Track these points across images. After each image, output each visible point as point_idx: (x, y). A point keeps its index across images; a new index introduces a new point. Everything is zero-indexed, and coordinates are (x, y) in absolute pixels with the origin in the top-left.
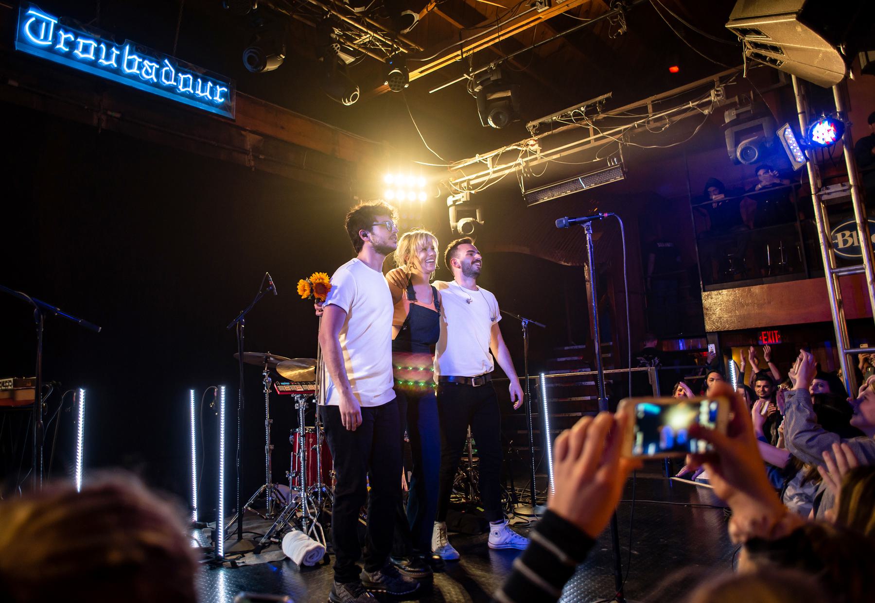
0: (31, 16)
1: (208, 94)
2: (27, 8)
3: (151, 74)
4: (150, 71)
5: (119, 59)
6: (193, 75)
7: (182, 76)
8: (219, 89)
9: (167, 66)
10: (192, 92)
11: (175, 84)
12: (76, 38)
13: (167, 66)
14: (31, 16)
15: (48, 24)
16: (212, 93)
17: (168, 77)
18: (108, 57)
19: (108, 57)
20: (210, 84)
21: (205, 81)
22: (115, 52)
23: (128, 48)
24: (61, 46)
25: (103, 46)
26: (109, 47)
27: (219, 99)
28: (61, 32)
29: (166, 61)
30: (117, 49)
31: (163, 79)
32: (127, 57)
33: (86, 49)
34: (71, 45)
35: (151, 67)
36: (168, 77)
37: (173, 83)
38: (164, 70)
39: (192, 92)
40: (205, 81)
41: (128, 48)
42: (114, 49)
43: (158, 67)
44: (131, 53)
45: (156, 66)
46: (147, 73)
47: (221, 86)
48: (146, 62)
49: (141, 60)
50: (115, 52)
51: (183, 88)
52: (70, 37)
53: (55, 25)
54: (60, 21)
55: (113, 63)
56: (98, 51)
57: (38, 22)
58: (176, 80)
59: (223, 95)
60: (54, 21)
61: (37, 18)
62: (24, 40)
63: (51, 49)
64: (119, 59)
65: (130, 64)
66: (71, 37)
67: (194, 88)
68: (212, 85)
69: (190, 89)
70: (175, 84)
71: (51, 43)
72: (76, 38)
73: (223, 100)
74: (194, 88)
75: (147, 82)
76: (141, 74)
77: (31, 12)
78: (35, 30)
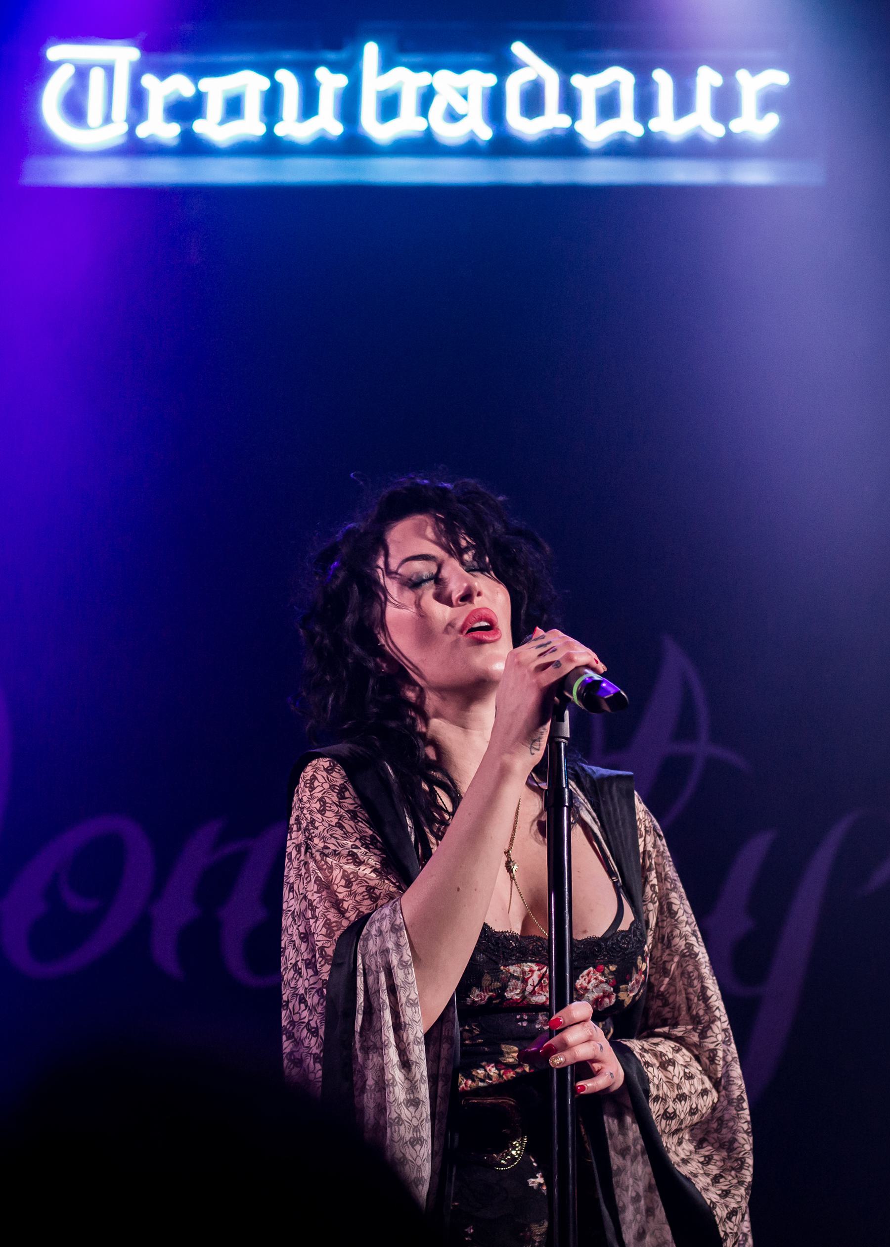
2: (41, 42)
4: (460, 107)
6: (629, 65)
9: (525, 65)
11: (564, 121)
12: (196, 84)
14: (55, 66)
18: (309, 107)
19: (309, 107)
23: (371, 51)
25: (286, 78)
28: (149, 81)
29: (519, 49)
30: (335, 67)
38: (515, 84)
39: (636, 131)
41: (371, 51)
42: (322, 74)
43: (491, 79)
44: (386, 65)
46: (453, 116)
47: (755, 68)
49: (424, 78)
54: (147, 48)
57: (82, 74)
70: (564, 121)
72: (195, 80)
73: (772, 121)
76: (429, 132)
77: (55, 52)
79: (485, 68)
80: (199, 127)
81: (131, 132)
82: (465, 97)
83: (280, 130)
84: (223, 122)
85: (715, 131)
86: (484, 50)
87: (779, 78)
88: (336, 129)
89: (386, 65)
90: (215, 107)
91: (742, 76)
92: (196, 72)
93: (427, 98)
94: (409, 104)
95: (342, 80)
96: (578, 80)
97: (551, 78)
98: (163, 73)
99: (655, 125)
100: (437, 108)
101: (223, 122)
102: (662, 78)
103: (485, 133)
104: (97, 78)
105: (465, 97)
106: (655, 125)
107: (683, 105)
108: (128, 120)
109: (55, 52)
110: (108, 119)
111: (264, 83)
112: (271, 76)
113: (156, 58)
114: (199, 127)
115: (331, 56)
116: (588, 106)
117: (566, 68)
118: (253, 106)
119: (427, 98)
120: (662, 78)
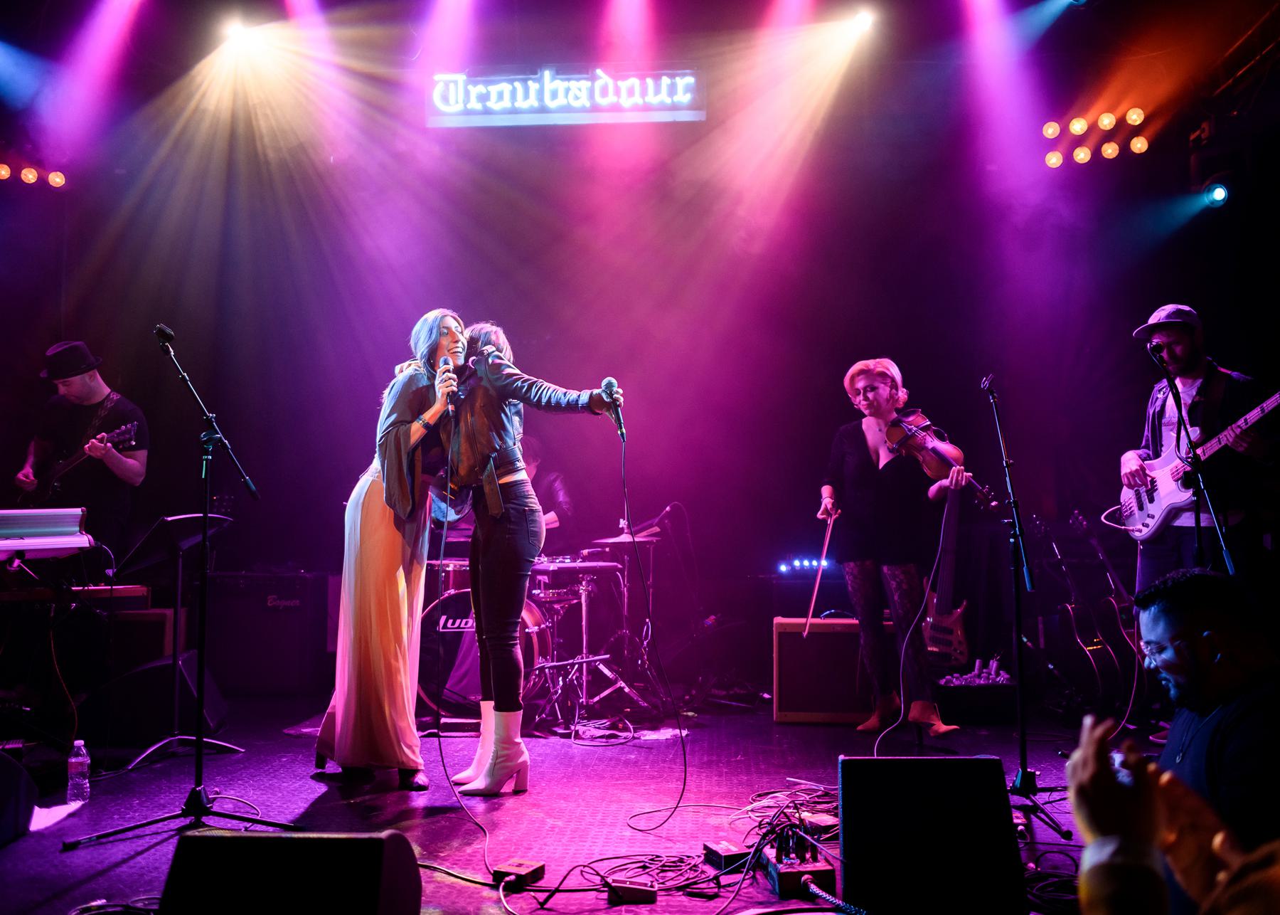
0: (438, 82)
2: (433, 73)
5: (541, 93)
7: (624, 85)
9: (600, 78)
13: (600, 78)
14: (438, 82)
15: (456, 82)
16: (672, 90)
17: (604, 92)
18: (526, 96)
19: (526, 96)
21: (657, 78)
24: (475, 105)
25: (517, 84)
26: (525, 81)
27: (684, 98)
28: (470, 87)
30: (534, 80)
33: (500, 96)
34: (484, 98)
35: (580, 90)
36: (604, 92)
37: (611, 99)
40: (657, 78)
41: (547, 74)
42: (530, 83)
43: (588, 84)
44: (553, 79)
45: (585, 84)
46: (577, 98)
47: (684, 75)
48: (573, 84)
49: (566, 84)
50: (533, 86)
52: (477, 94)
54: (469, 75)
55: (533, 102)
57: (447, 84)
58: (617, 92)
59: (688, 89)
60: (461, 78)
62: (439, 113)
63: (468, 113)
64: (541, 93)
65: (554, 95)
66: (481, 89)
67: (644, 93)
69: (637, 100)
74: (644, 93)
75: (583, 110)
78: (445, 99)
79: (587, 79)
81: (465, 105)
84: (496, 102)
85: (668, 101)
86: (587, 73)
88: (536, 104)
89: (553, 79)
90: (494, 97)
93: (568, 91)
94: (561, 94)
96: (620, 83)
97: (610, 82)
98: (475, 84)
100: (571, 95)
101: (496, 102)
102: (650, 81)
103: (588, 104)
104: (452, 86)
108: (464, 101)
109: (437, 77)
110: (457, 102)
112: (513, 85)
113: (473, 79)
115: (532, 76)
116: (624, 93)
118: (507, 96)
119: (568, 91)
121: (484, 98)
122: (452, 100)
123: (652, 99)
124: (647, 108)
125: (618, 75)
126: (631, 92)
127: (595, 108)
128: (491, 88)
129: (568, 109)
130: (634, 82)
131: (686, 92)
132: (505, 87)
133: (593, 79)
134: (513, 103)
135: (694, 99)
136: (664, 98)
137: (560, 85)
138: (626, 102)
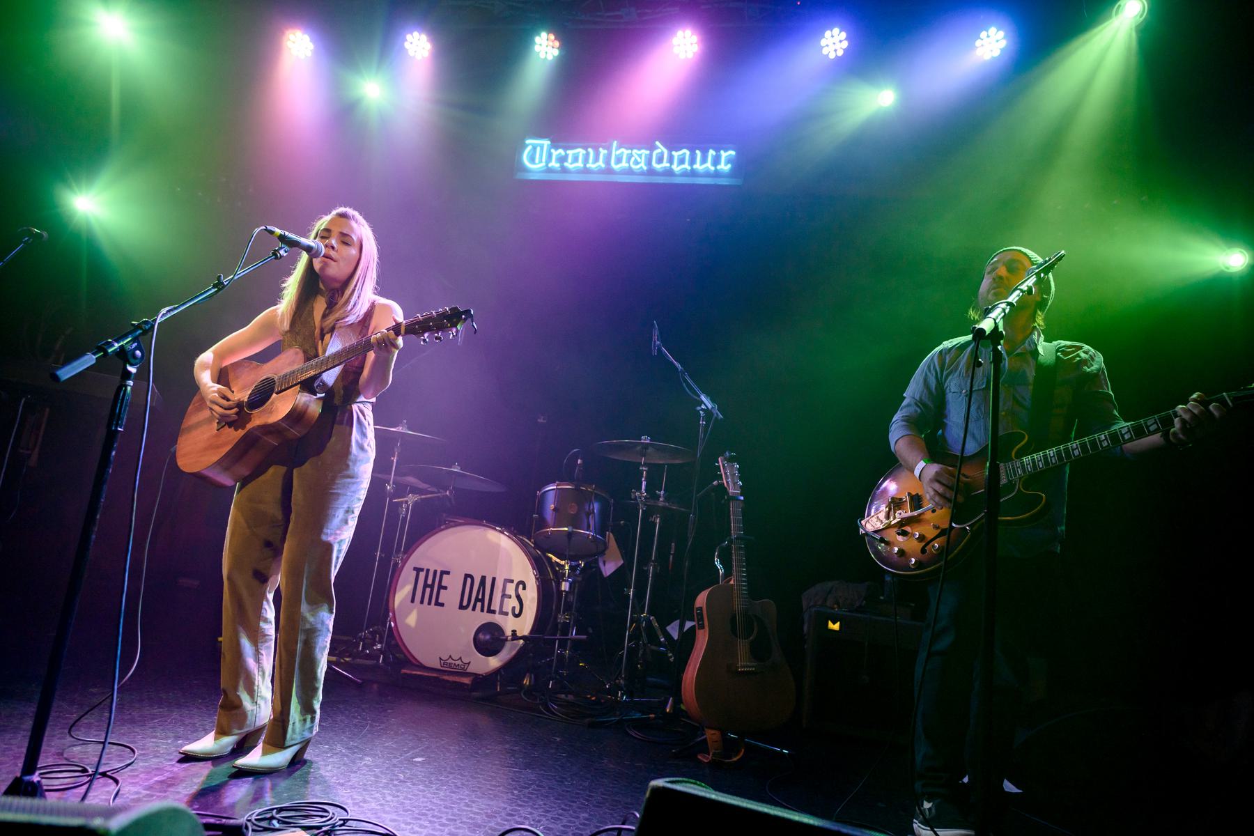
1: (709, 165)
3: (640, 163)
4: (639, 160)
5: (607, 161)
8: (724, 155)
9: (658, 148)
10: (689, 168)
13: (658, 148)
14: (528, 145)
16: (716, 161)
17: (660, 160)
18: (596, 159)
19: (596, 159)
20: (712, 152)
22: (603, 152)
23: (615, 144)
24: (554, 164)
25: (590, 150)
27: (725, 167)
28: (553, 151)
29: (658, 143)
30: (604, 148)
31: (654, 164)
32: (615, 153)
33: (576, 159)
34: (562, 160)
35: (640, 156)
36: (660, 160)
37: (665, 164)
38: (655, 153)
41: (615, 144)
42: (601, 149)
43: (648, 152)
45: (645, 152)
46: (636, 163)
47: (726, 150)
48: (635, 152)
49: (629, 151)
50: (603, 152)
51: (677, 166)
52: (560, 154)
53: (548, 145)
54: (552, 141)
56: (586, 160)
58: (671, 160)
59: (728, 161)
61: (532, 144)
64: (607, 161)
65: (619, 160)
66: (561, 151)
67: (693, 161)
68: (714, 153)
69: (687, 166)
70: (668, 165)
71: (544, 164)
72: (565, 151)
74: (693, 161)
79: (646, 149)
80: (566, 164)
81: (547, 165)
82: (641, 158)
83: (588, 166)
87: (733, 153)
88: (603, 166)
89: (619, 147)
90: (570, 159)
91: (722, 152)
92: (565, 148)
95: (606, 152)
96: (674, 153)
97: (666, 152)
98: (557, 148)
99: (695, 167)
100: (632, 160)
101: (571, 164)
102: (698, 152)
104: (538, 149)
105: (641, 158)
106: (695, 167)
107: (704, 161)
110: (541, 161)
111: (584, 152)
114: (566, 164)
115: (603, 144)
117: (671, 148)
118: (581, 158)
120: (698, 152)
121: (562, 160)
122: (537, 160)
123: (698, 166)
124: (693, 173)
125: (672, 145)
126: (682, 161)
127: (651, 172)
128: (568, 152)
129: (630, 172)
130: (686, 152)
131: (726, 165)
132: (581, 152)
133: (652, 148)
134: (585, 165)
135: (732, 170)
136: (709, 165)
137: (625, 152)
138: (676, 168)
